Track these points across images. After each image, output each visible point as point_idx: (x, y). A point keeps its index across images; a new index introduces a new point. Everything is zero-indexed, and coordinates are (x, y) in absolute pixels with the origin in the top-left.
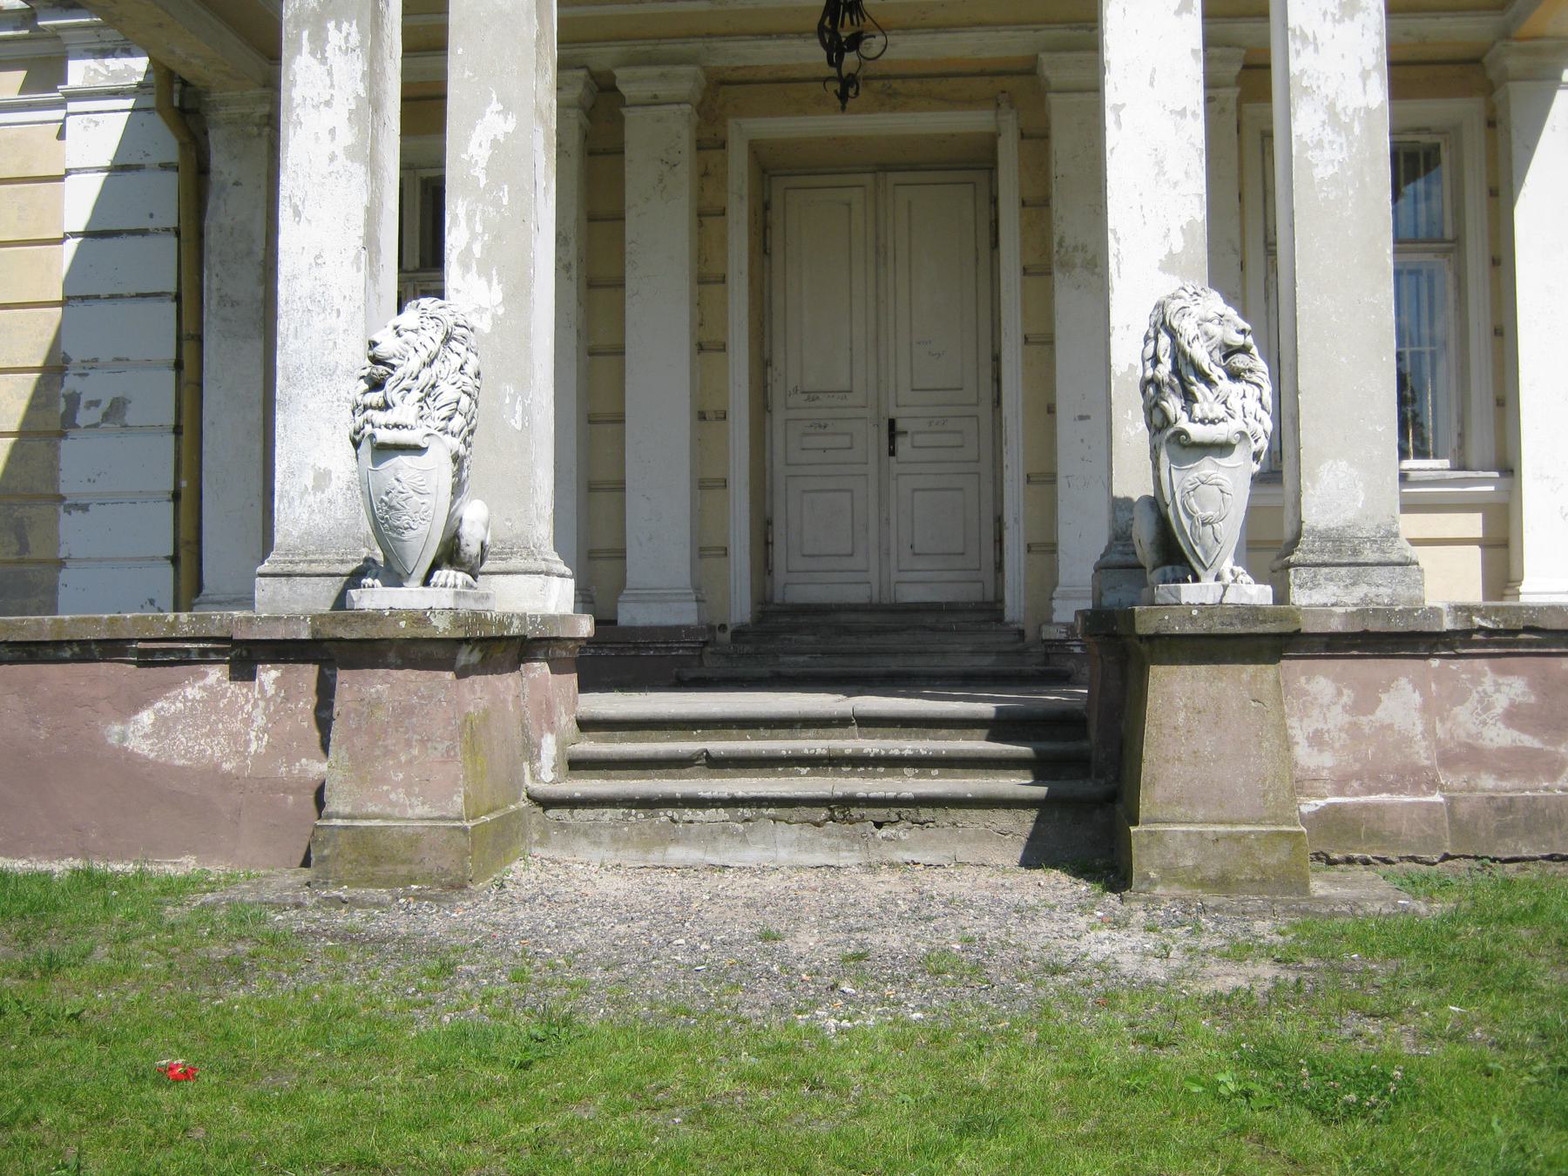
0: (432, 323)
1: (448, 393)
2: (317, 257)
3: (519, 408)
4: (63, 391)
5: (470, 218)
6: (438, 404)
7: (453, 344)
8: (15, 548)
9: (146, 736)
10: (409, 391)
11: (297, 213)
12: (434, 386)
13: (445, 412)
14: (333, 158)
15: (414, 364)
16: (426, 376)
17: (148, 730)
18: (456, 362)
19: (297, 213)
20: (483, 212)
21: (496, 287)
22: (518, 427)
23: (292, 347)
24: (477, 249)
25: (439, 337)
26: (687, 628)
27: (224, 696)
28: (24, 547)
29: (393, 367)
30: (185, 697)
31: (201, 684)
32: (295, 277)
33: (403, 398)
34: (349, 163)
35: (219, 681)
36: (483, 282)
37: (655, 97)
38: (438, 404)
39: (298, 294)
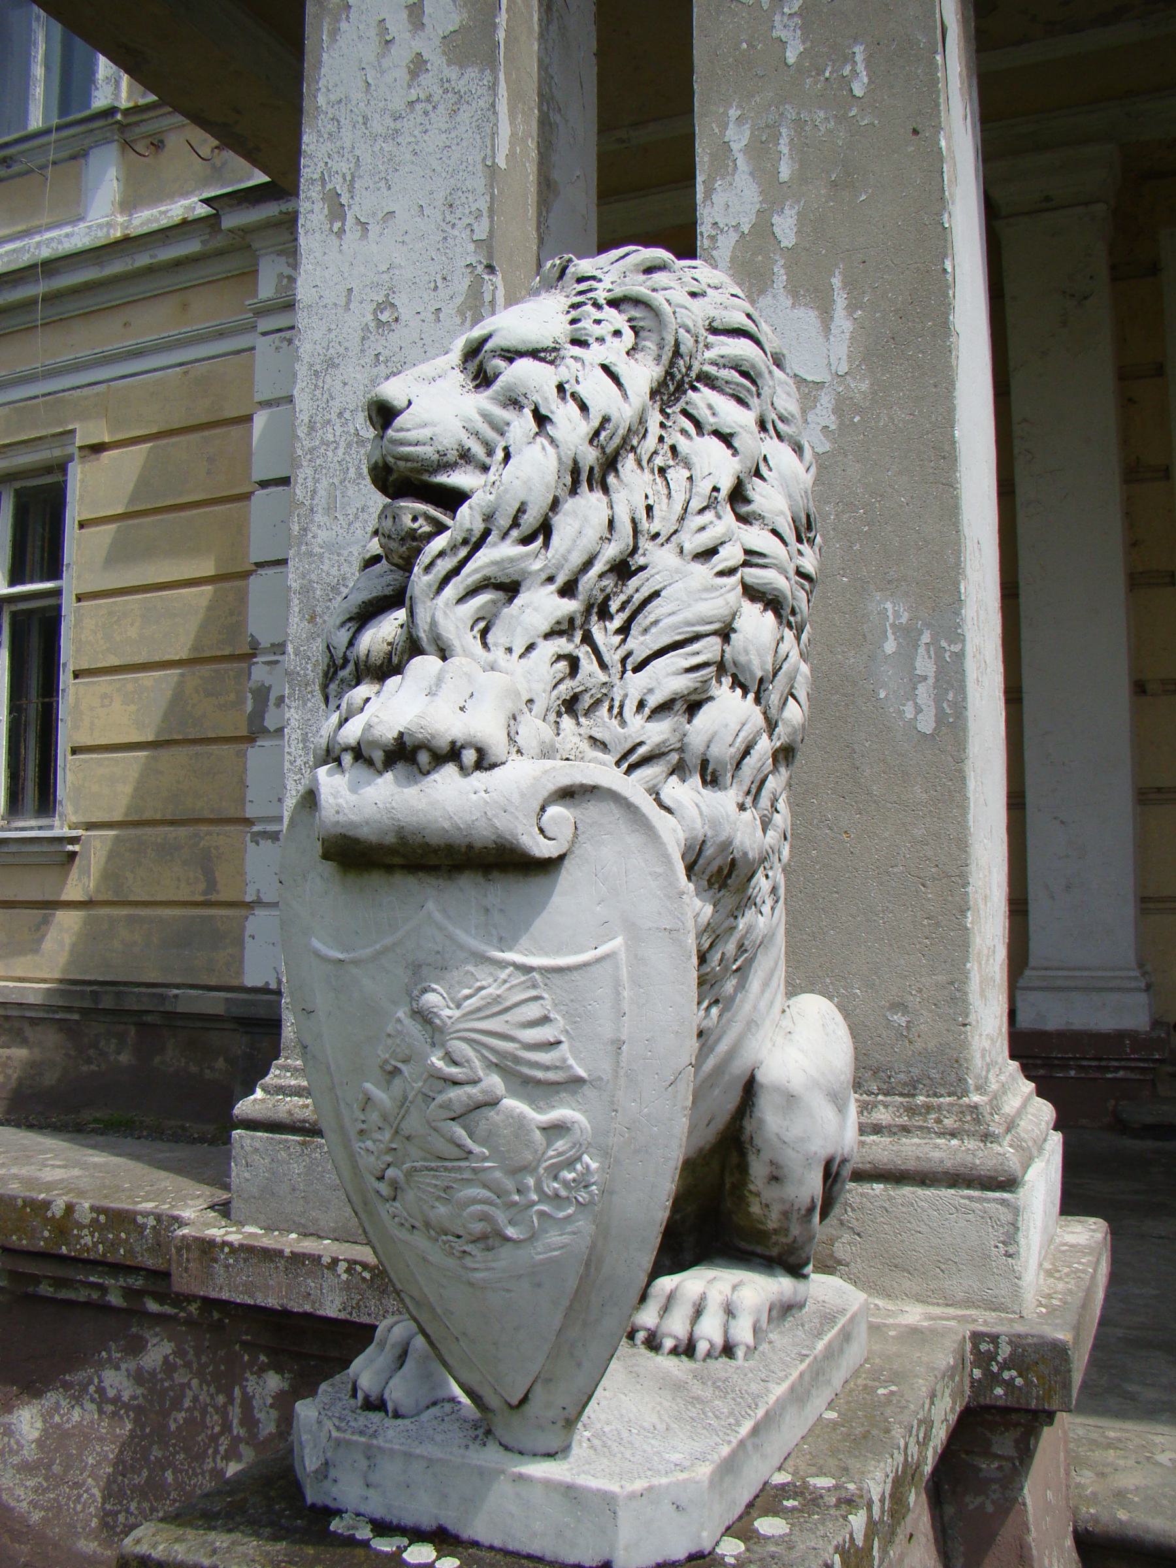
0: (616, 319)
1: (685, 593)
2: (380, 308)
3: (925, 665)
4: (252, 684)
5: (762, 151)
6: (640, 644)
7: (702, 399)
8: (202, 886)
9: (27, 1468)
10: (510, 589)
11: (337, 211)
12: (623, 570)
13: (668, 678)
14: (418, 66)
15: (532, 470)
16: (582, 523)
17: (30, 1453)
18: (717, 466)
19: (337, 211)
20: (799, 124)
21: (842, 322)
22: (927, 724)
23: (323, 535)
24: (786, 227)
25: (642, 374)
26: (1132, 1035)
27: (177, 1404)
28: (212, 885)
29: (453, 499)
30: (101, 1390)
31: (130, 1365)
32: (331, 364)
33: (485, 629)
34: (452, 73)
35: (168, 1367)
36: (809, 317)
37: (1048, 199)
38: (640, 644)
39: (336, 405)
